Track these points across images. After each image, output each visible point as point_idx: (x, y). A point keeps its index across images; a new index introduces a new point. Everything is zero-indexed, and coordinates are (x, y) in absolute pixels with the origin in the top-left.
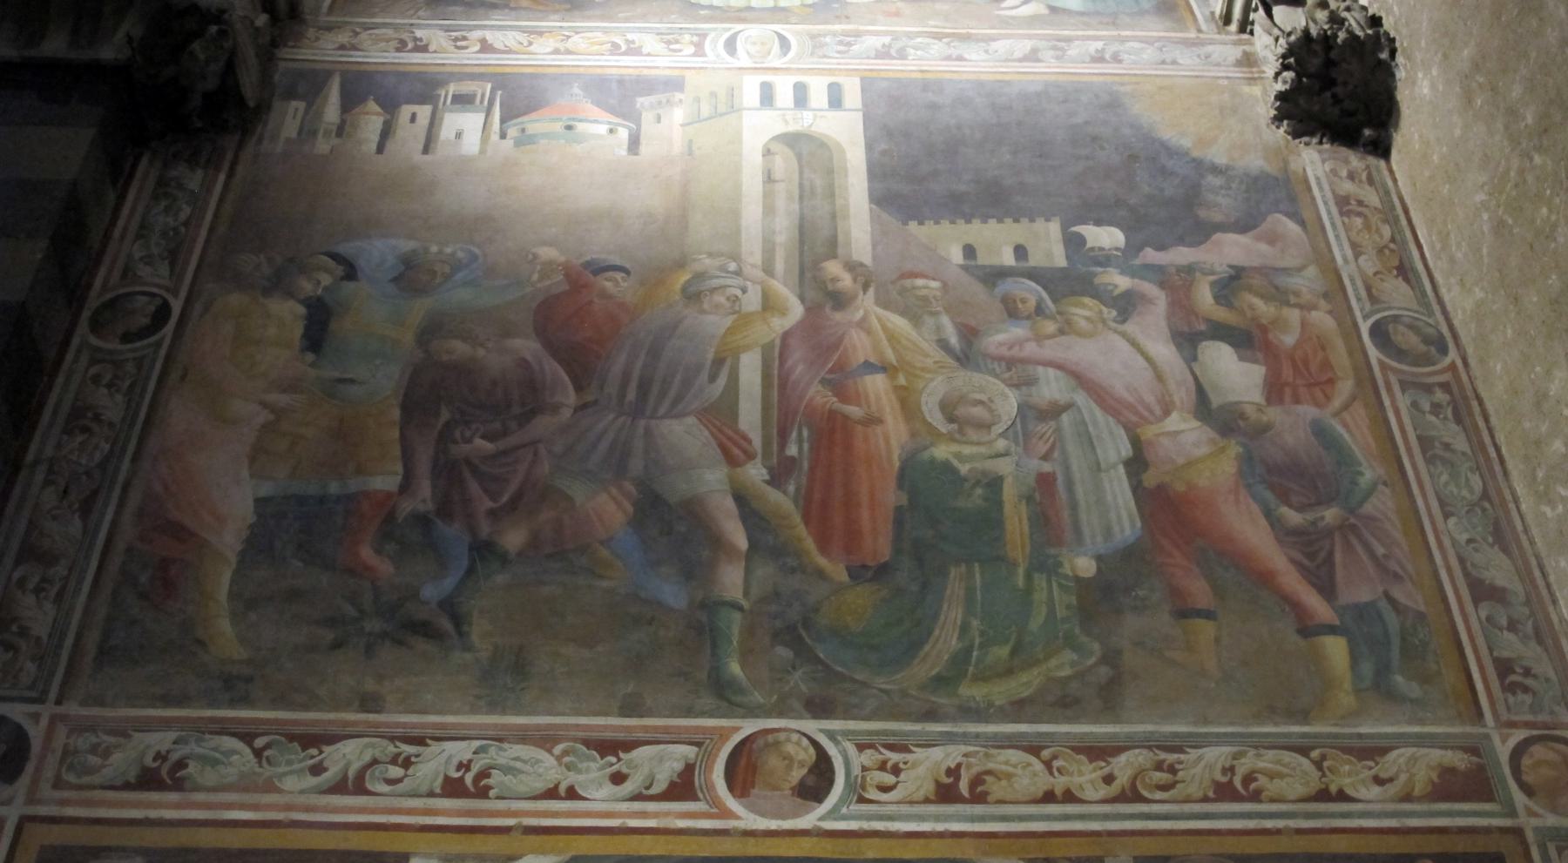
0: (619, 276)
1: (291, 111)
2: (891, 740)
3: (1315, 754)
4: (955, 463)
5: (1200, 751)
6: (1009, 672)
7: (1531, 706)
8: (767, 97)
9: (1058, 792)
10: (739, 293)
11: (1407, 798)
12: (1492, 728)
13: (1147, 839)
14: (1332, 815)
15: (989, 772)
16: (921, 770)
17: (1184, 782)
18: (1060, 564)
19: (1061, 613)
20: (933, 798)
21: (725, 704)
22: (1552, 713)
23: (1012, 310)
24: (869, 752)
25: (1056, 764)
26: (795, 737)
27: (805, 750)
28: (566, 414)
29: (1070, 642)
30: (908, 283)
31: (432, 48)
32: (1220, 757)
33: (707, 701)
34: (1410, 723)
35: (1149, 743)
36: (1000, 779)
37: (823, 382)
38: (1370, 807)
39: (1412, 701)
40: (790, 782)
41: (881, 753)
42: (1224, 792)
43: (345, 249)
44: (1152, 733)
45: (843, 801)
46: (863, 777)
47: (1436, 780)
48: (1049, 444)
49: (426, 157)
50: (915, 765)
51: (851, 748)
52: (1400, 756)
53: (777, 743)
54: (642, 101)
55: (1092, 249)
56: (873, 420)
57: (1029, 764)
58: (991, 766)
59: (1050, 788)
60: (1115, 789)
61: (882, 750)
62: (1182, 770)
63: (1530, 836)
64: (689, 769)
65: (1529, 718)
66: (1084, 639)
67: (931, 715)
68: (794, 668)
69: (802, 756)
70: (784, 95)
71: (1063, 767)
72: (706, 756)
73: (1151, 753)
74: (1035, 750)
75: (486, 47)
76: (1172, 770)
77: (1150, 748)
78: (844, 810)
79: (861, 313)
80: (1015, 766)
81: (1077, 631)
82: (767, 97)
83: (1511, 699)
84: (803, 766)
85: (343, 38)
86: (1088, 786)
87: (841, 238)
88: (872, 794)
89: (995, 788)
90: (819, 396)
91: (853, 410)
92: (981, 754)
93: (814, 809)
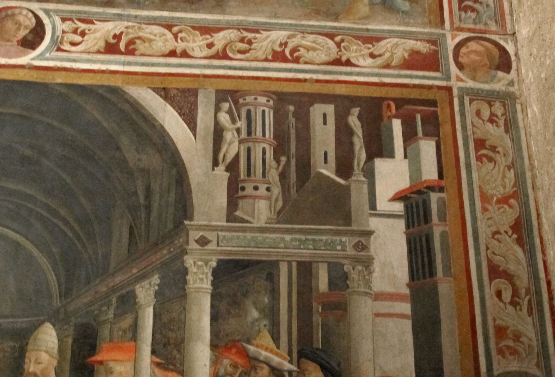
2: (83, 16)
3: (338, 39)
5: (269, 33)
7: (474, 19)
9: (178, 51)
11: (387, 66)
12: (448, 31)
13: (226, 80)
14: (341, 73)
15: (139, 38)
16: (98, 35)
17: (255, 49)
20: (102, 50)
22: (486, 24)
24: (68, 23)
25: (180, 35)
26: (25, 12)
27: (30, 19)
32: (281, 36)
34: (399, 25)
35: (239, 27)
36: (144, 42)
38: (364, 70)
39: (403, 12)
40: (17, 38)
41: (75, 23)
42: (278, 56)
44: (242, 21)
45: (47, 50)
46: (63, 37)
47: (406, 57)
50: (95, 32)
52: (388, 43)
53: (13, 15)
57: (164, 35)
58: (141, 34)
59: (174, 48)
61: (76, 21)
62: (256, 43)
63: (455, 92)
65: (472, 26)
69: (27, 23)
71: (185, 37)
73: (239, 33)
74: (169, 27)
76: (250, 42)
77: (239, 29)
78: (48, 55)
80: (155, 35)
83: (463, 14)
84: (27, 28)
86: (197, 50)
88: (66, 47)
89: (141, 47)
92: (136, 28)
93: (30, 53)
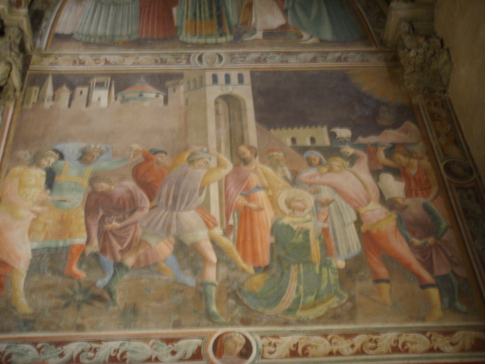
0: (163, 155)
1: (34, 92)
4: (291, 225)
6: (314, 306)
8: (215, 79)
9: (334, 351)
10: (208, 160)
18: (331, 264)
19: (332, 282)
21: (211, 323)
23: (310, 164)
28: (147, 211)
29: (336, 293)
30: (271, 154)
31: (86, 63)
33: (205, 321)
35: (367, 332)
37: (242, 194)
43: (59, 147)
46: (263, 349)
48: (326, 216)
49: (87, 109)
51: (258, 338)
54: (168, 83)
55: (339, 138)
56: (260, 209)
58: (309, 342)
60: (355, 349)
64: (199, 348)
66: (341, 292)
67: (286, 323)
68: (236, 308)
70: (221, 78)
72: (205, 343)
73: (368, 336)
74: (325, 336)
75: (107, 62)
79: (253, 167)
81: (339, 289)
82: (215, 79)
85: (51, 60)
87: (245, 136)
89: (311, 351)
90: (240, 200)
91: (253, 205)
